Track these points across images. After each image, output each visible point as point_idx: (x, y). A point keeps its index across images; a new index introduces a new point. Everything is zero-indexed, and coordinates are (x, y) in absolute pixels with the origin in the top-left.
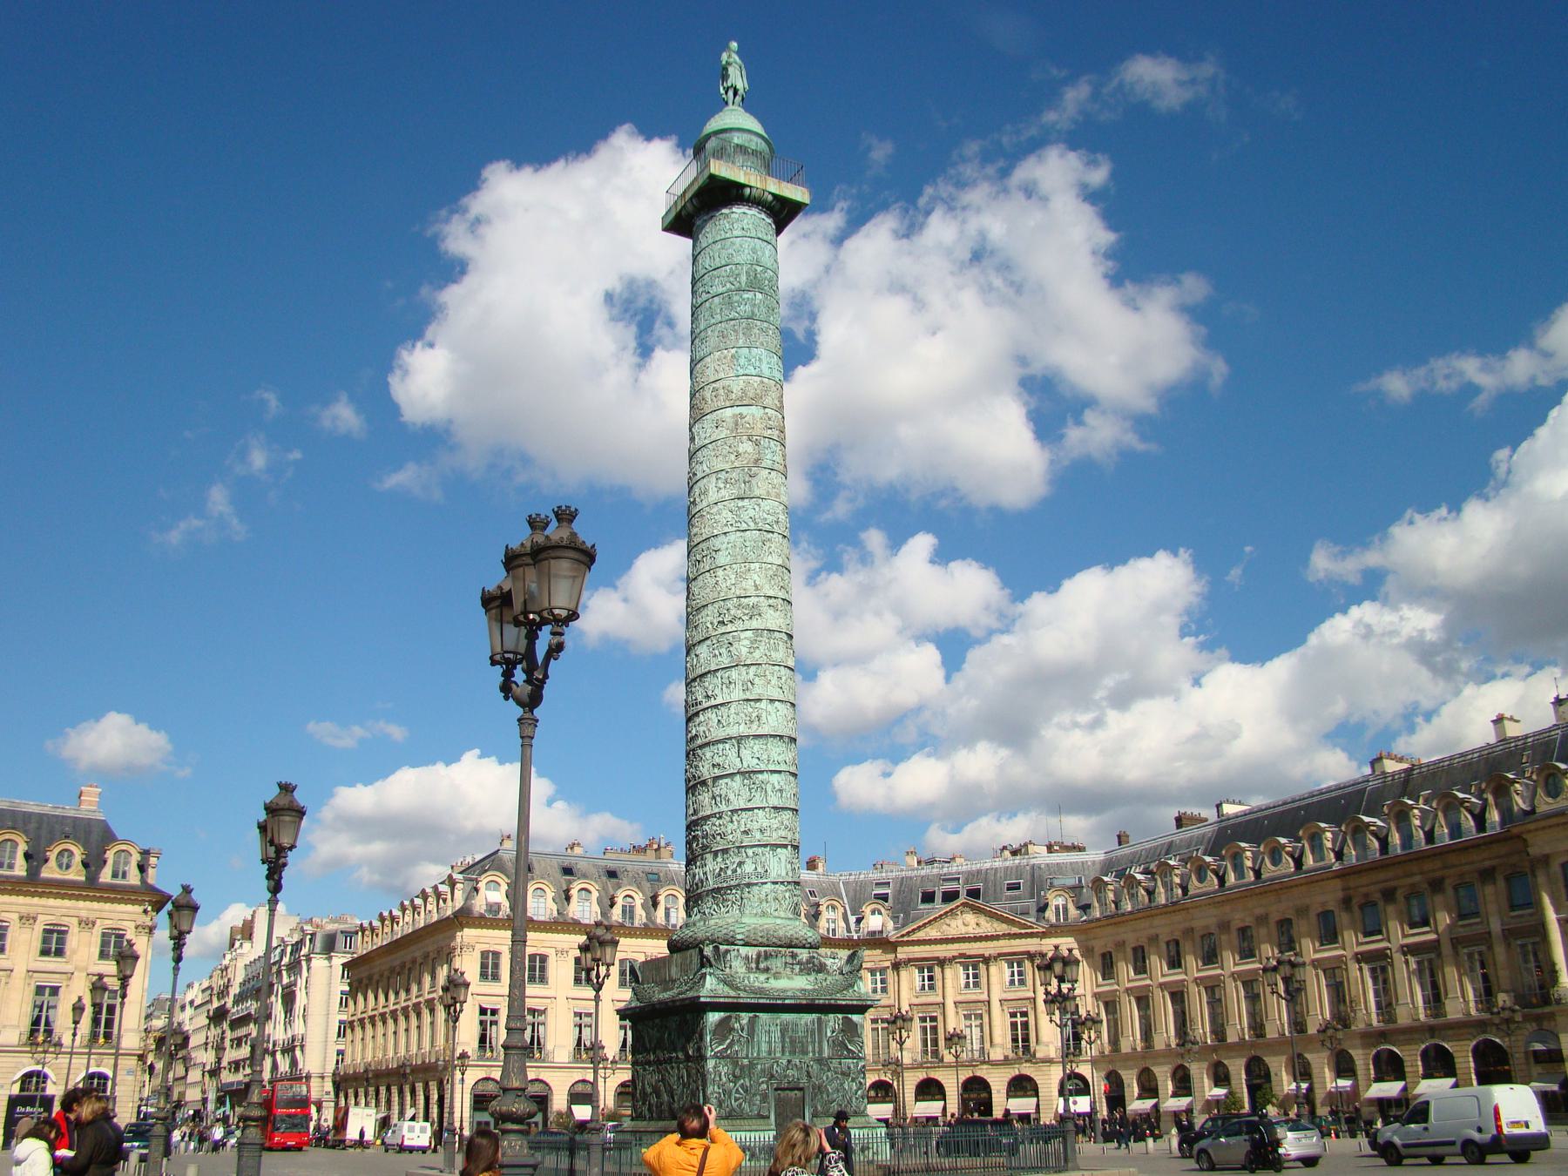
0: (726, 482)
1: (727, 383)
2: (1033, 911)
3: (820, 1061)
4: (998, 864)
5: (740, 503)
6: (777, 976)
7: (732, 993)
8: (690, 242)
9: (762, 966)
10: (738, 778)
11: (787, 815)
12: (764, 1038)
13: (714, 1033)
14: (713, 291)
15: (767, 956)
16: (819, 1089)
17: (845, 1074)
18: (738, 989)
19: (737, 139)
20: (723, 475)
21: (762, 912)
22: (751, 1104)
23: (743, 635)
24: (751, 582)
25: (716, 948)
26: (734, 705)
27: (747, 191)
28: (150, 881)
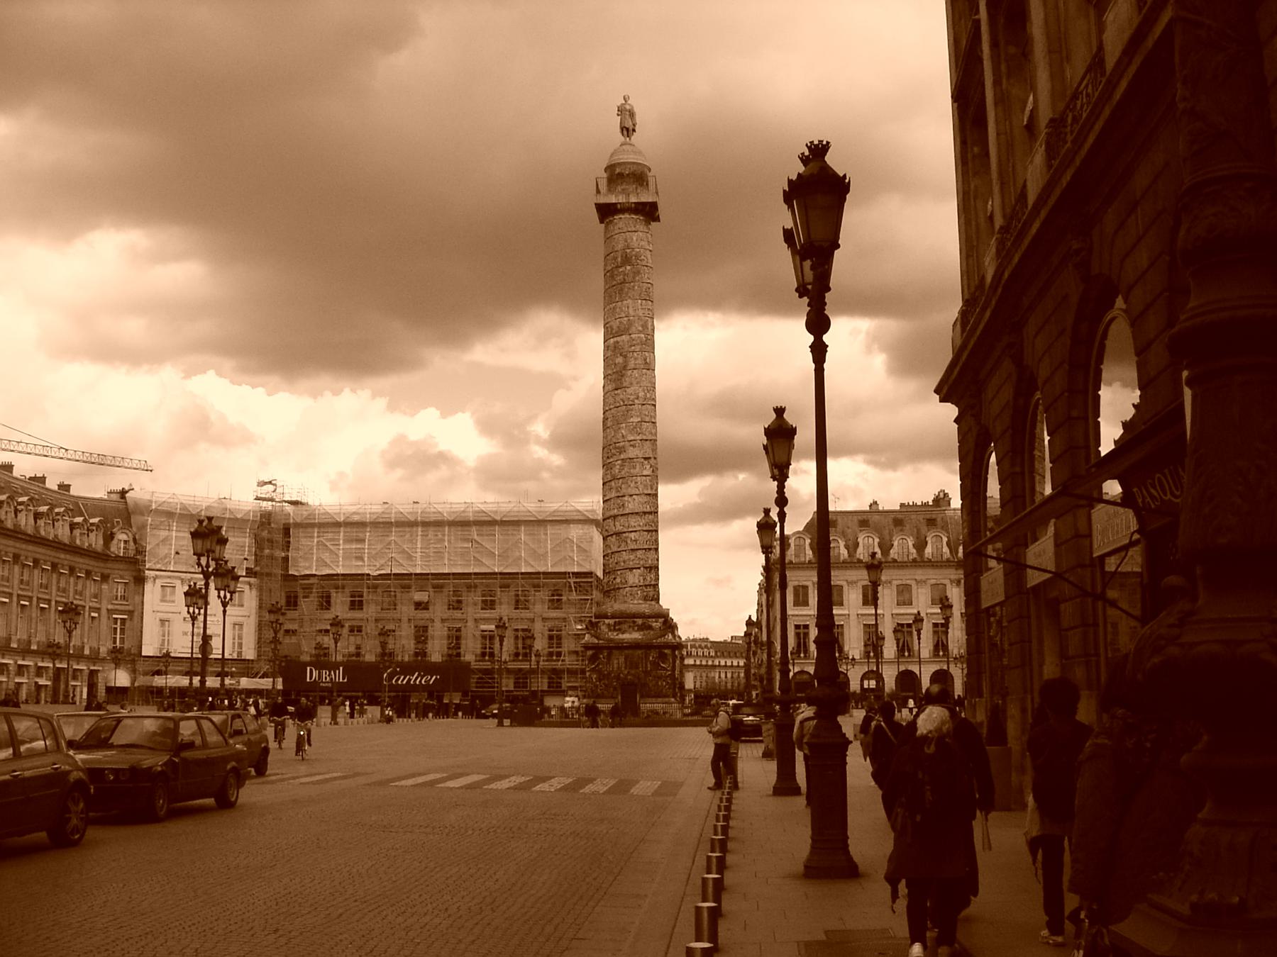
15: (620, 623)
17: (660, 678)
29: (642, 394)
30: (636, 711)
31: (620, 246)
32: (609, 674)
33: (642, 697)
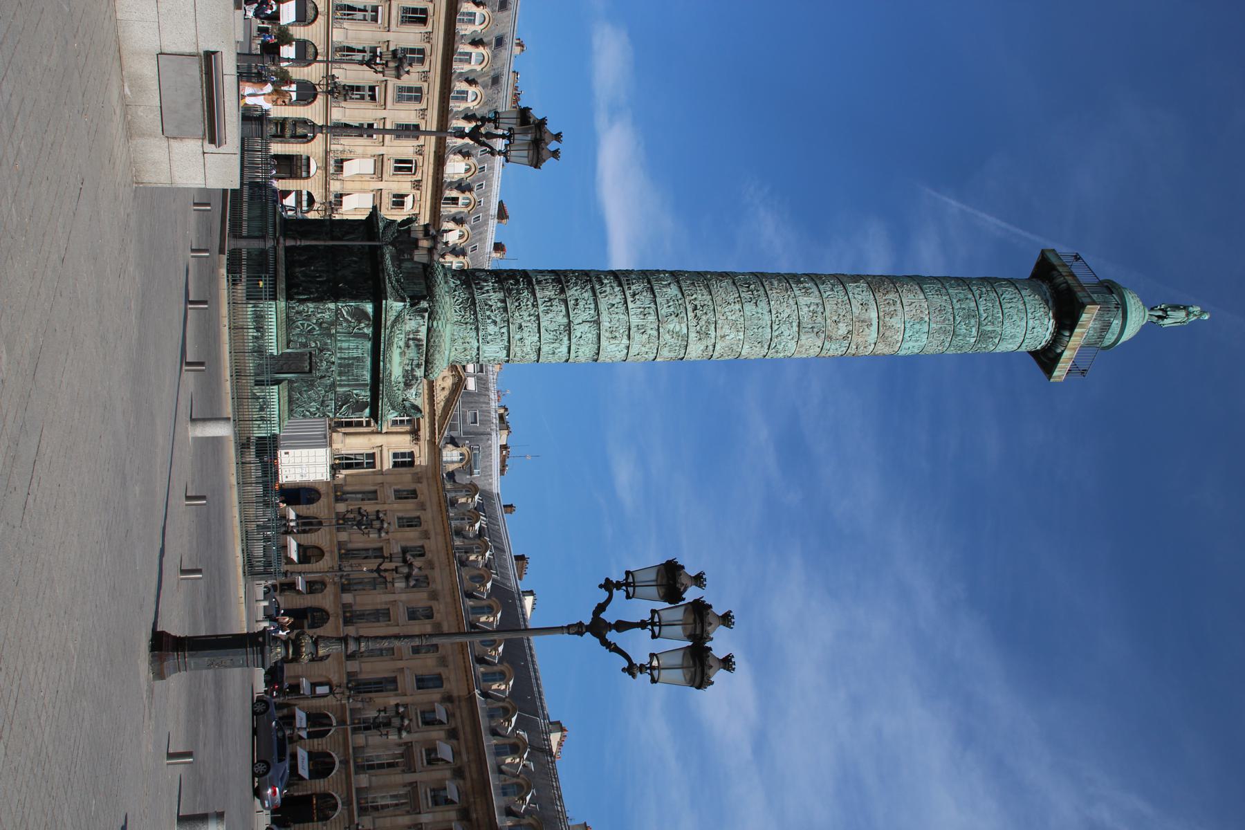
0: (814, 312)
1: (900, 313)
2: (454, 434)
3: (333, 385)
4: (494, 405)
5: (795, 324)
6: (402, 354)
7: (389, 323)
8: (1028, 275)
9: (411, 342)
10: (565, 320)
11: (533, 357)
12: (352, 345)
13: (357, 308)
14: (982, 302)
15: (418, 346)
16: (311, 385)
18: (393, 326)
19: (1116, 323)
20: (820, 309)
21: (454, 337)
22: (299, 335)
23: (684, 326)
24: (728, 332)
25: (426, 310)
26: (626, 318)
27: (1067, 334)
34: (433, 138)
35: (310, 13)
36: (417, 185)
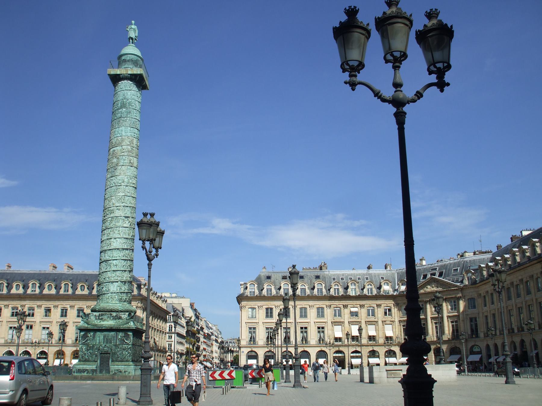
7: (87, 326)
13: (82, 337)
15: (102, 315)
16: (115, 354)
28: (141, 293)
29: (126, 180)
30: (108, 371)
31: (121, 98)
32: (93, 346)
33: (113, 361)
34: (297, 303)
35: (253, 354)
36: (345, 306)
